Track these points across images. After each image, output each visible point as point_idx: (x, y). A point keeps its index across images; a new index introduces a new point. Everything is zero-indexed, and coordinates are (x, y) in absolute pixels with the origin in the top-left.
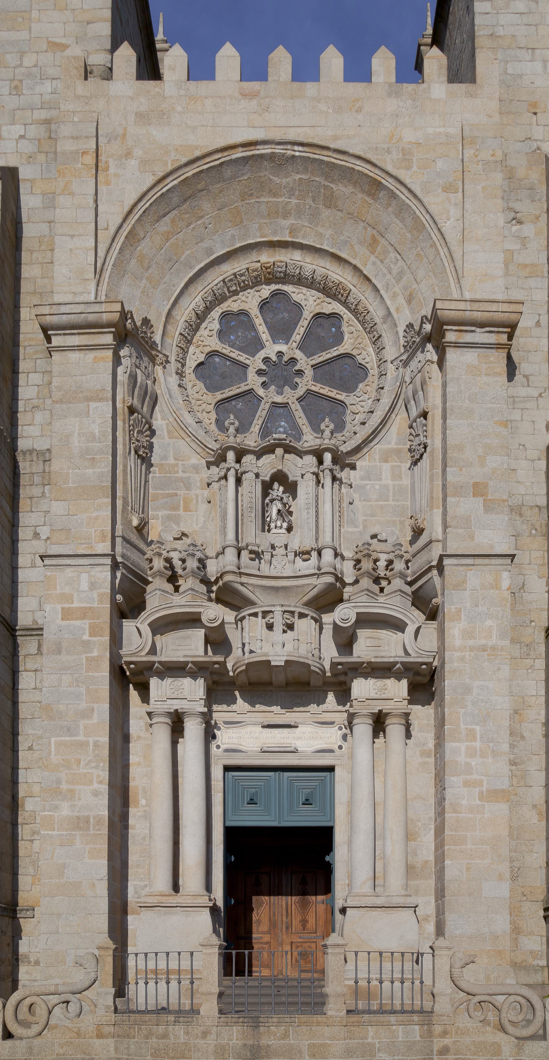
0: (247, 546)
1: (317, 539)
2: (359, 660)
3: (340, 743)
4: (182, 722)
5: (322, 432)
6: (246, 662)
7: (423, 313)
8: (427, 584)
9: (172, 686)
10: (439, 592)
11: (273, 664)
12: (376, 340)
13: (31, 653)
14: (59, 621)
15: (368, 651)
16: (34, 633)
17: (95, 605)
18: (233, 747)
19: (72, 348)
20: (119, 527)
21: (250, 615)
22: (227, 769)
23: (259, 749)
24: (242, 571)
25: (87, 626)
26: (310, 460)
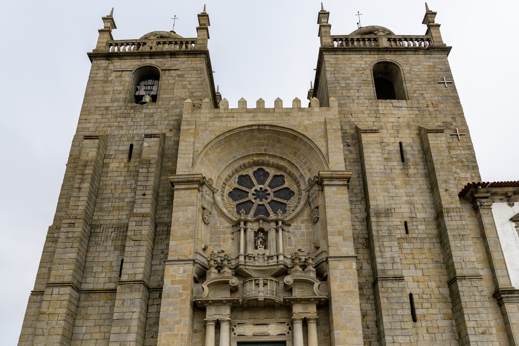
2: (295, 297)
3: (288, 331)
5: (278, 214)
7: (315, 175)
12: (298, 184)
14: (170, 286)
17: (185, 279)
18: (241, 334)
19: (182, 189)
21: (249, 281)
25: (181, 287)
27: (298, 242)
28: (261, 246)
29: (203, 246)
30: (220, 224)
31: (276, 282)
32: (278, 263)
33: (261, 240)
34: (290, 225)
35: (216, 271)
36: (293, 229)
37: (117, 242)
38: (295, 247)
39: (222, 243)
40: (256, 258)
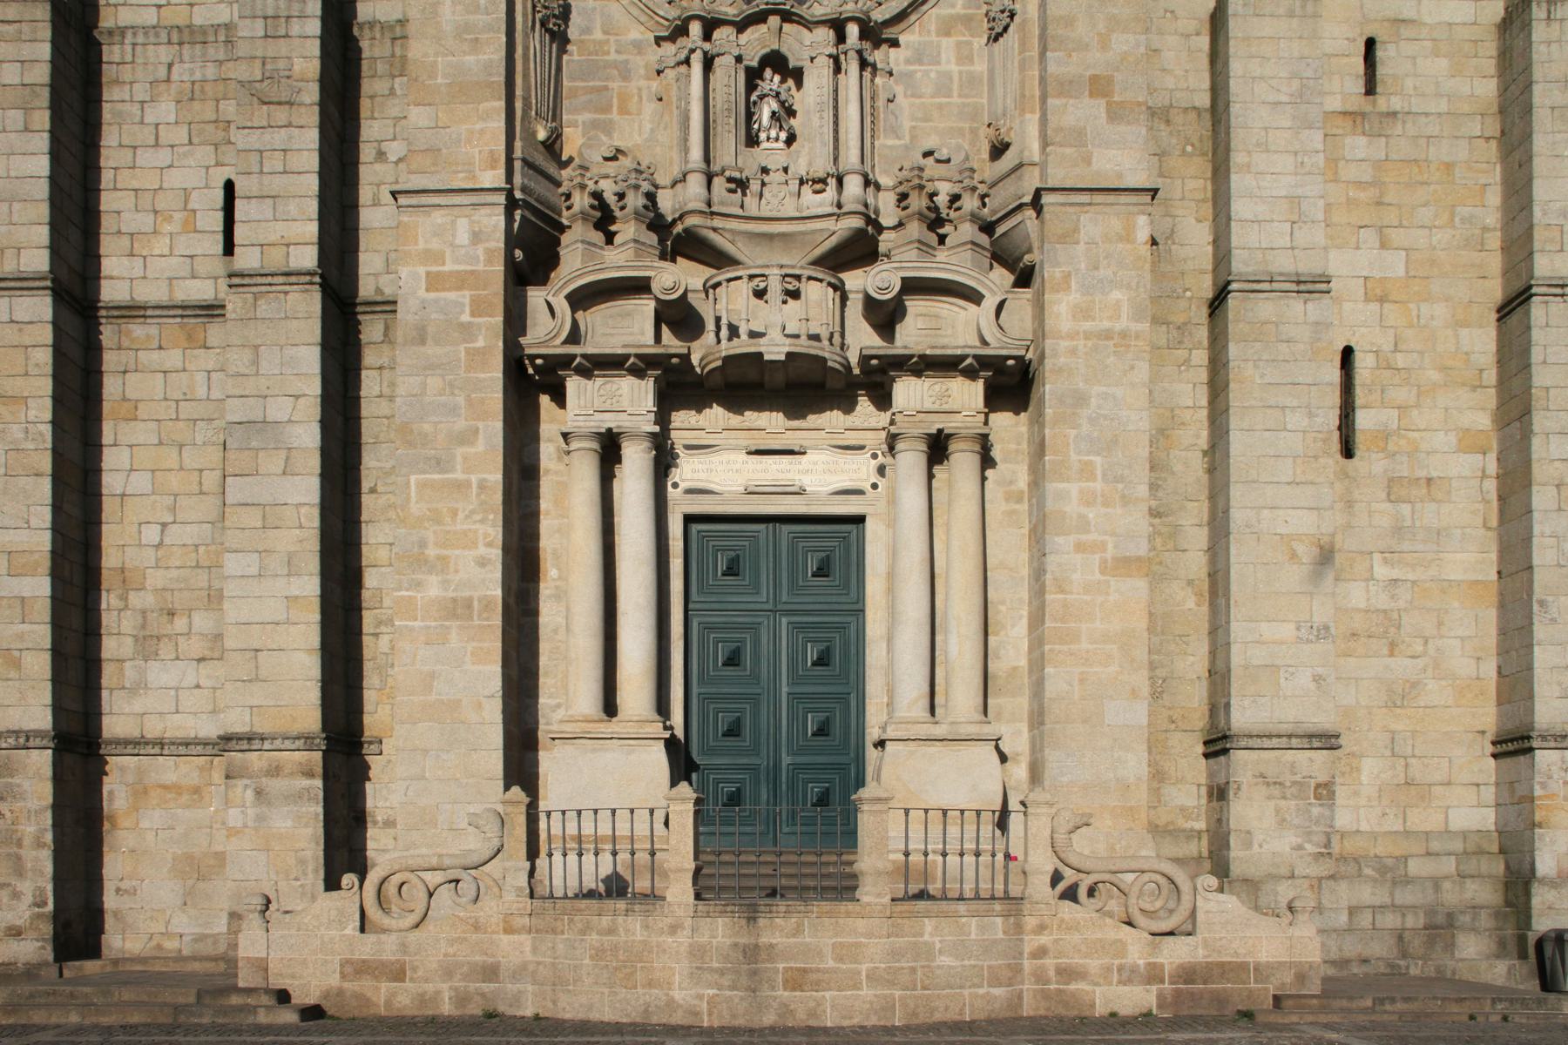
0: (723, 171)
1: (836, 159)
4: (619, 448)
6: (723, 354)
8: (1017, 230)
9: (602, 392)
10: (1036, 245)
11: (766, 357)
13: (374, 340)
15: (920, 336)
16: (378, 309)
20: (518, 144)
22: (689, 519)
23: (742, 489)
24: (714, 209)
26: (825, 35)
27: (926, 120)
28: (773, 134)
29: (542, 135)
30: (605, 33)
31: (830, 284)
32: (839, 206)
33: (775, 106)
34: (894, 43)
35: (598, 237)
36: (908, 62)
37: (196, 105)
38: (913, 138)
39: (615, 116)
40: (755, 186)
